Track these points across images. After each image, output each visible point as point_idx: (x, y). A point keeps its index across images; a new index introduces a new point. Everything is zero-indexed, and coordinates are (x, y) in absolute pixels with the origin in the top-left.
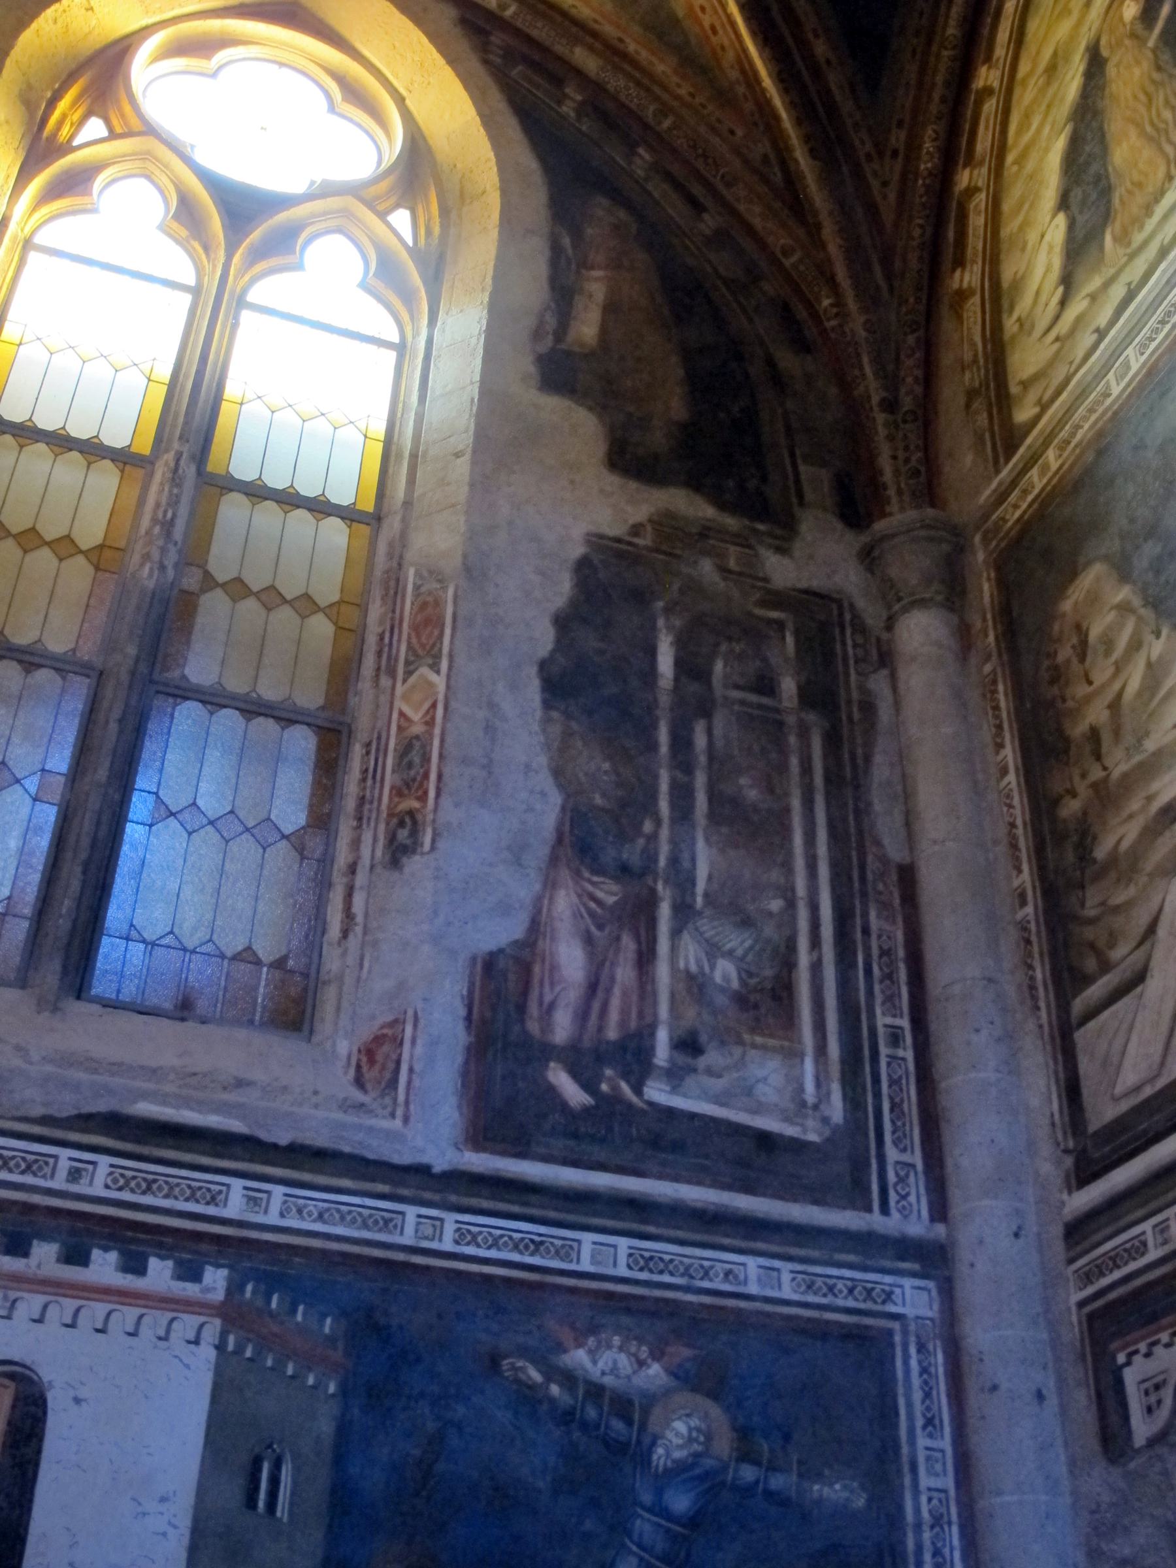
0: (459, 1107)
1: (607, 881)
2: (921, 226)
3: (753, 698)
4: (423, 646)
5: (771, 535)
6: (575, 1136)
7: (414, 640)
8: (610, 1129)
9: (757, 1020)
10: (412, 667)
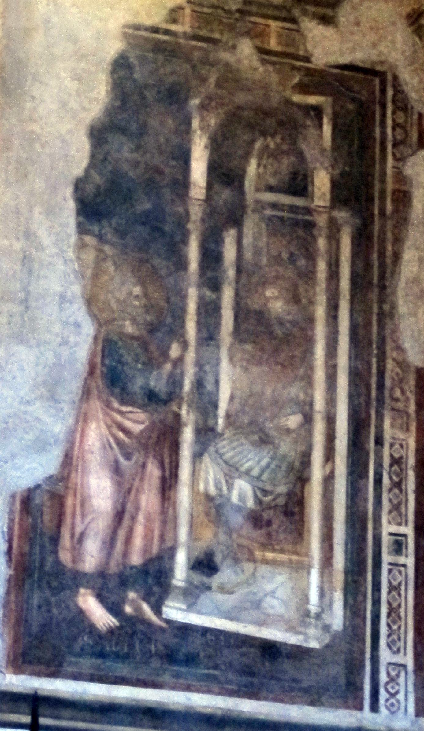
1: (135, 410)
3: (286, 199)
6: (102, 655)
8: (131, 646)
9: (269, 535)
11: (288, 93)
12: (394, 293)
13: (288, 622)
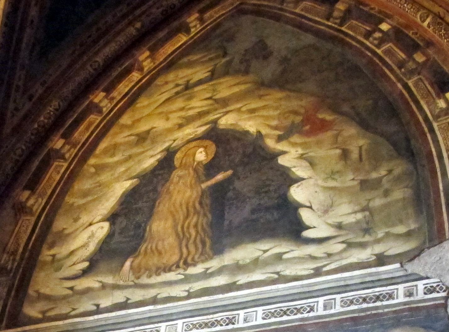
2: (23, 150)
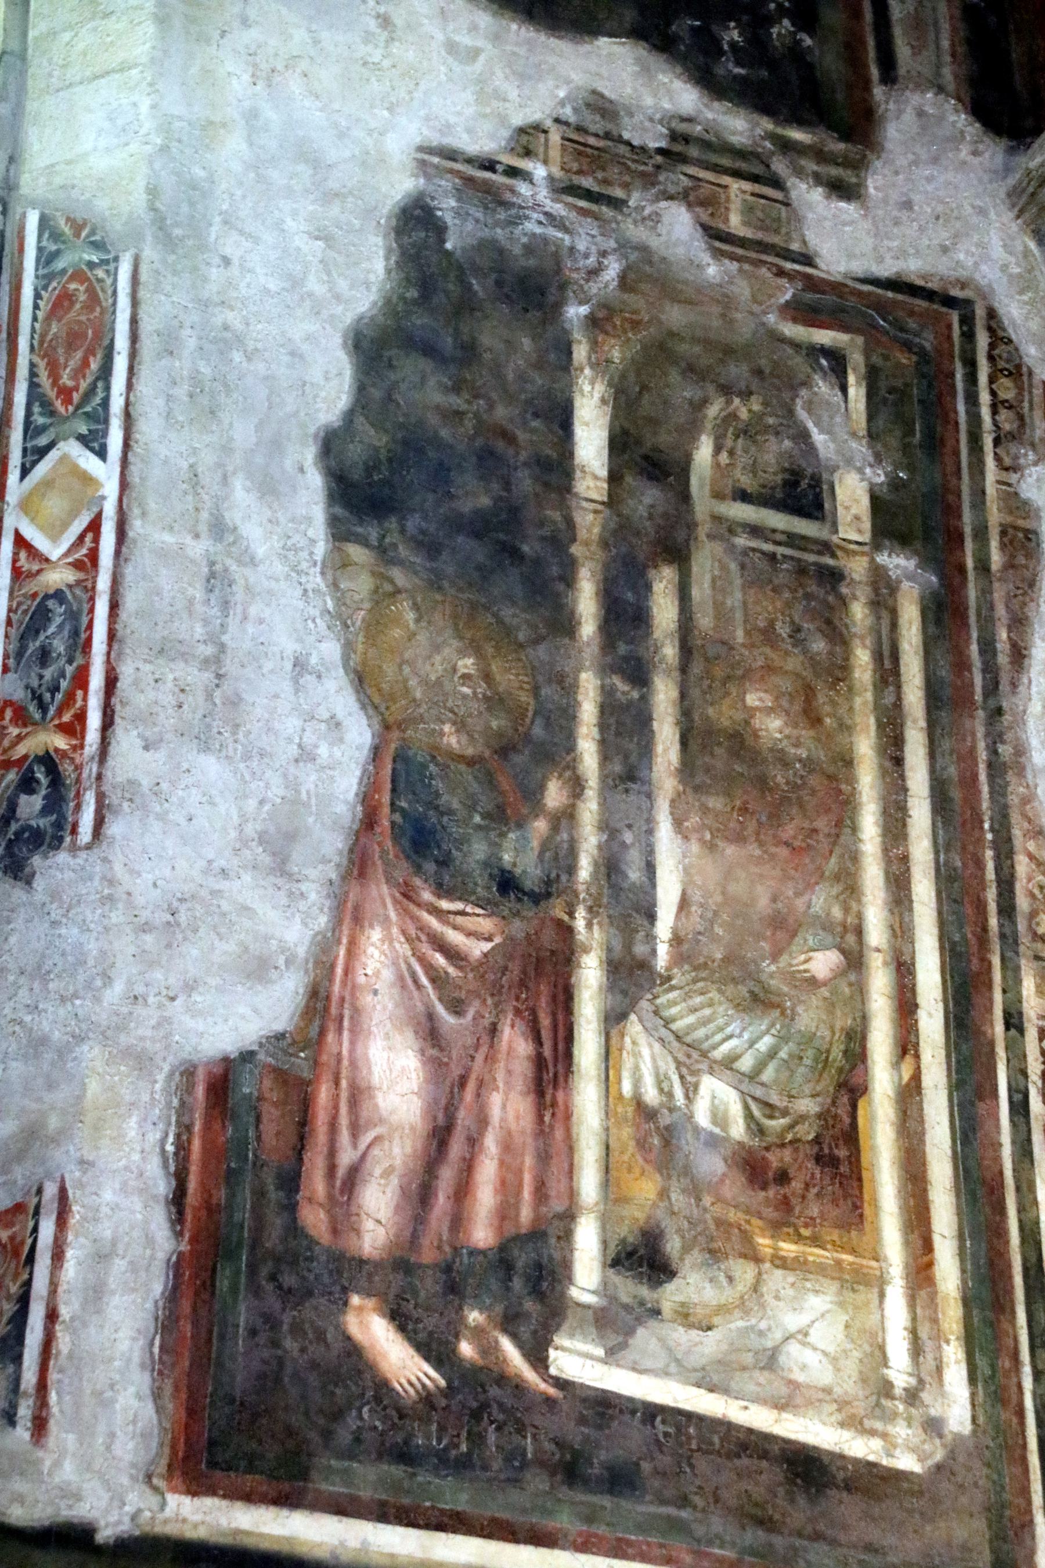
0: (157, 1395)
3: (778, 520)
4: (66, 394)
5: (820, 155)
6: (405, 1456)
7: (44, 379)
8: (477, 1439)
10: (43, 441)
11: (771, 318)
12: (1020, 720)
13: (842, 1404)
